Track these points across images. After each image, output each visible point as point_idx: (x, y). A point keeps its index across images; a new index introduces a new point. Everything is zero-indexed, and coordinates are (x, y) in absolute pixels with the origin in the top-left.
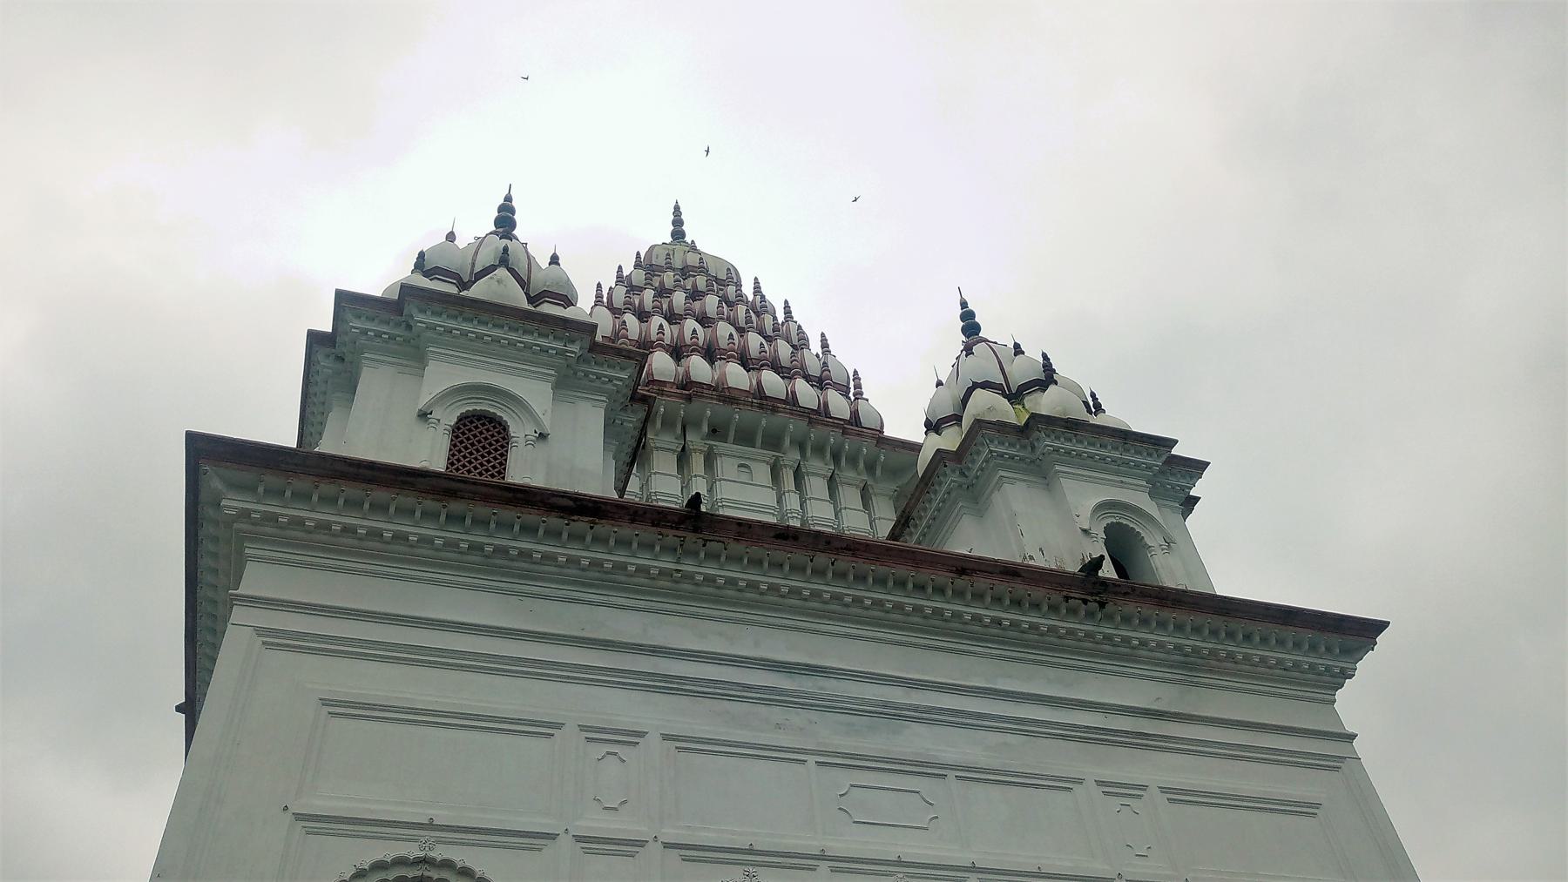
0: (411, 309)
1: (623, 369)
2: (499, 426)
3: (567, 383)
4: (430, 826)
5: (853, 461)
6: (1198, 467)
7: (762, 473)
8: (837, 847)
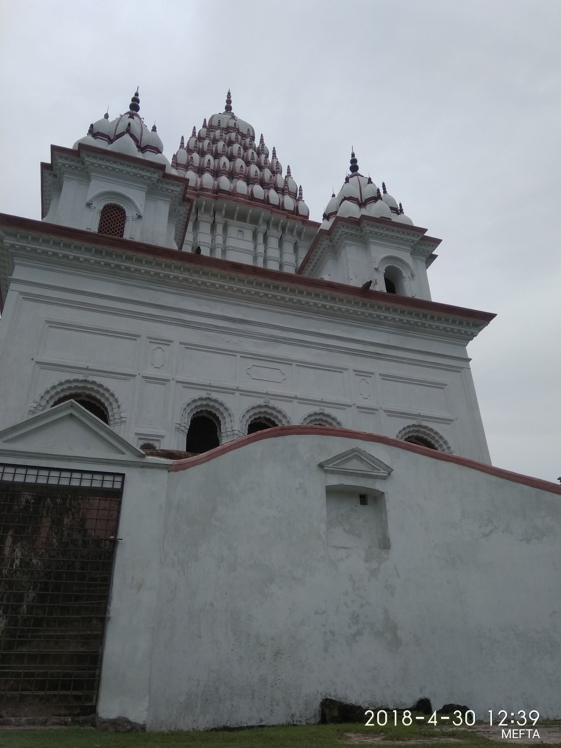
0: (83, 154)
1: (178, 186)
2: (122, 212)
3: (152, 192)
4: (87, 369)
5: (291, 231)
6: (437, 242)
7: (249, 235)
8: (243, 387)
